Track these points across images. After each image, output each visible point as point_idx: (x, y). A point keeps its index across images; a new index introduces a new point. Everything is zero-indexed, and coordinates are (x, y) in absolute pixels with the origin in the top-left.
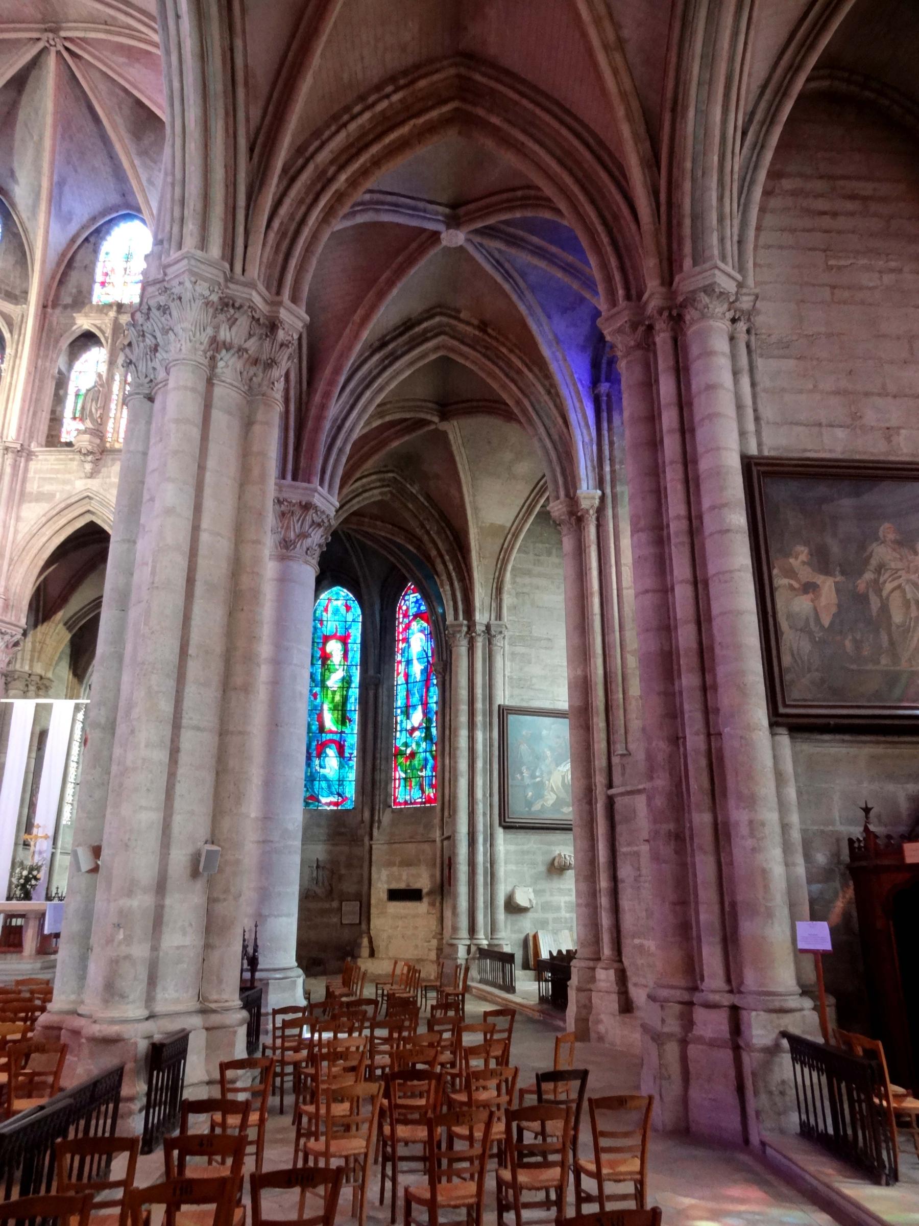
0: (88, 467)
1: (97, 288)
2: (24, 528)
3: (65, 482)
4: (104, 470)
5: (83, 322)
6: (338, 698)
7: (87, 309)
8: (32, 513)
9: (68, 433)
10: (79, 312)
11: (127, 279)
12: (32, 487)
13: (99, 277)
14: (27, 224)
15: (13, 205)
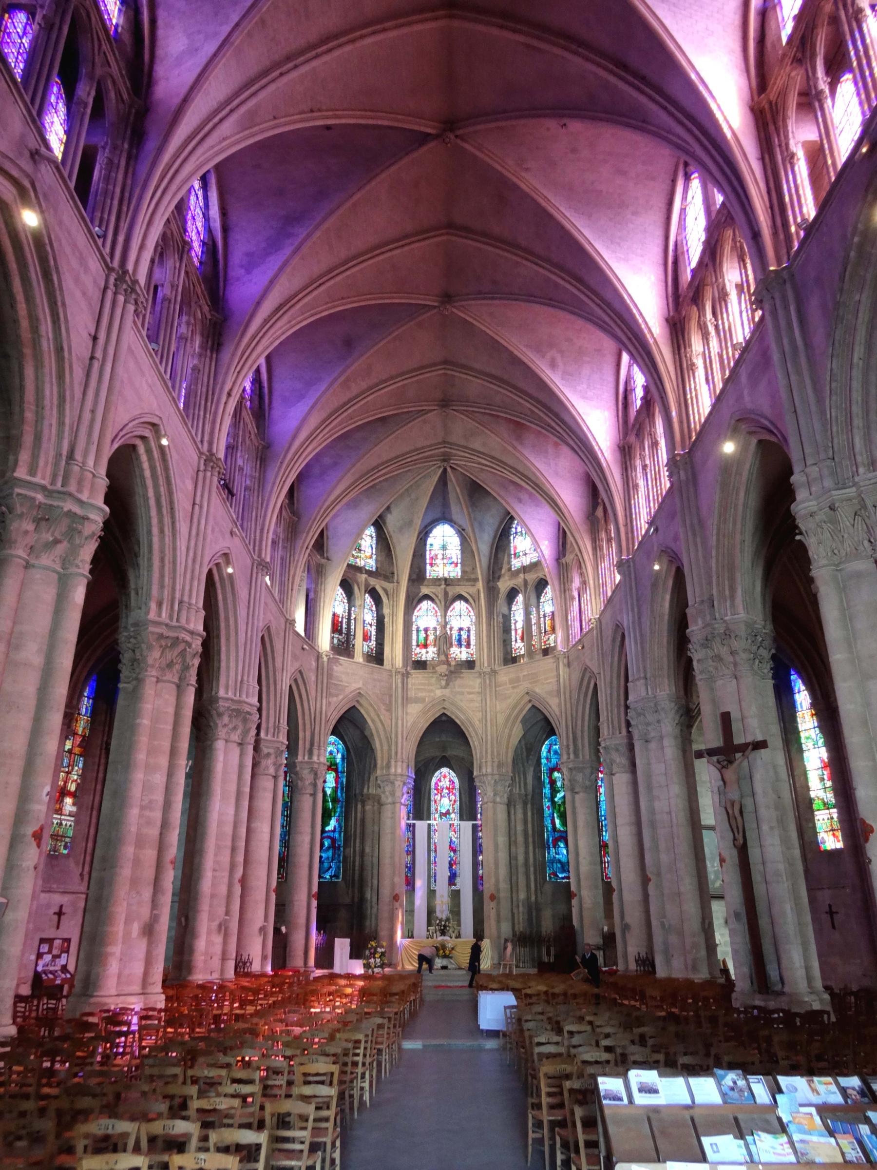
0: (443, 683)
1: (428, 567)
2: (410, 720)
3: (430, 691)
4: (451, 684)
5: (425, 590)
6: (562, 809)
7: (426, 583)
8: (414, 710)
9: (416, 655)
10: (422, 585)
11: (445, 561)
12: (412, 694)
13: (428, 561)
14: (392, 533)
15: (385, 523)
